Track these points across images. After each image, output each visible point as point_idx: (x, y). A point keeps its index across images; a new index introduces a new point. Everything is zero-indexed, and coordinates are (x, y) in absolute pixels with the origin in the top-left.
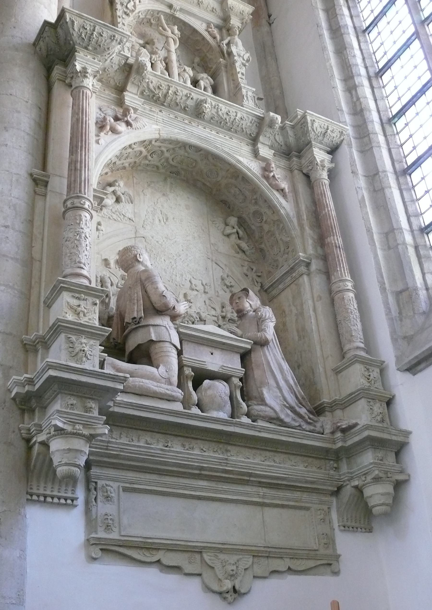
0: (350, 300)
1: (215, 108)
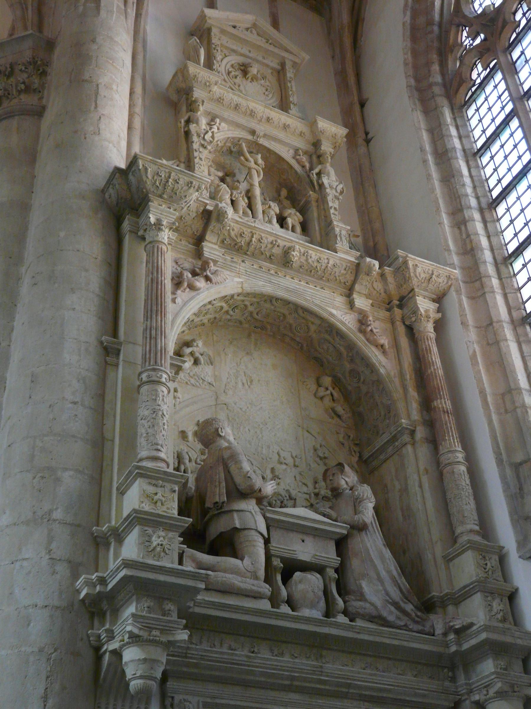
0: (461, 474)
1: (304, 255)
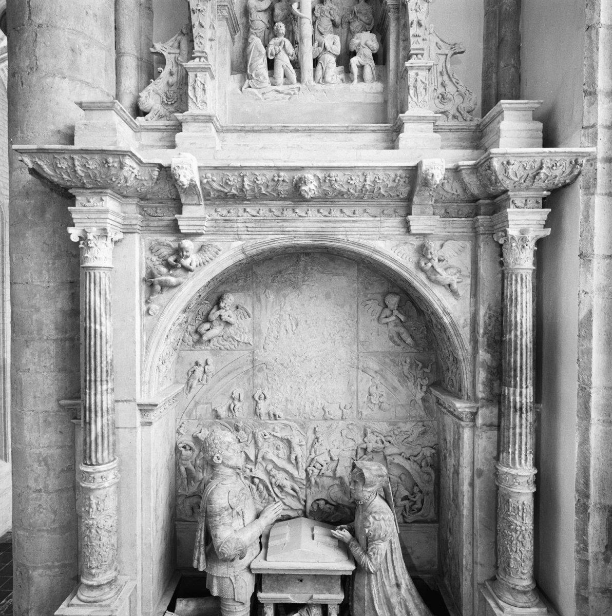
0: (518, 508)
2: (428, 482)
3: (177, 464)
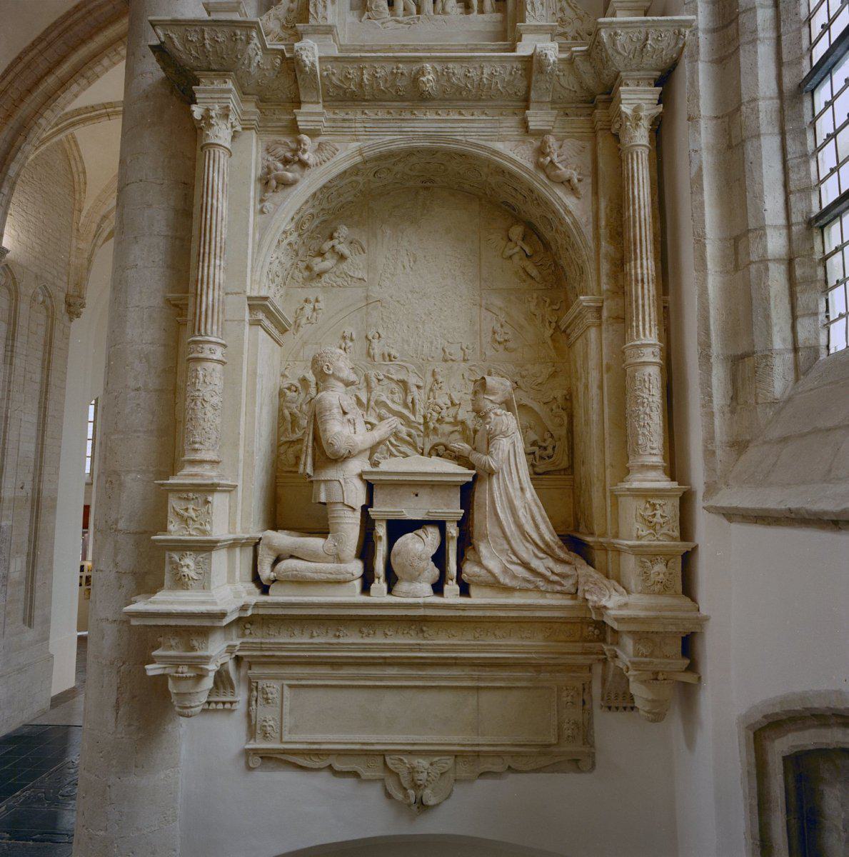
2: (561, 425)
3: (280, 410)
